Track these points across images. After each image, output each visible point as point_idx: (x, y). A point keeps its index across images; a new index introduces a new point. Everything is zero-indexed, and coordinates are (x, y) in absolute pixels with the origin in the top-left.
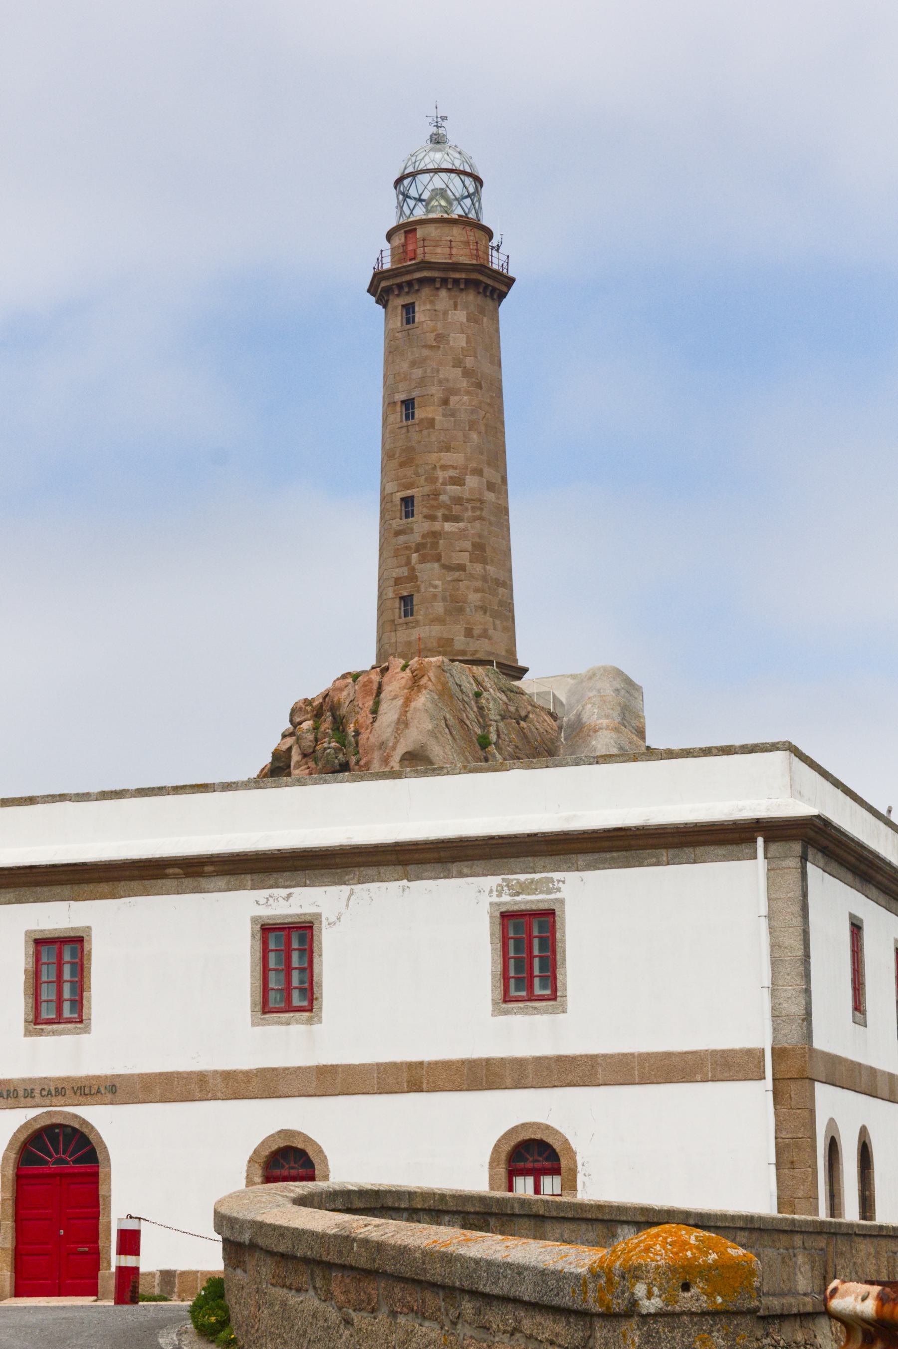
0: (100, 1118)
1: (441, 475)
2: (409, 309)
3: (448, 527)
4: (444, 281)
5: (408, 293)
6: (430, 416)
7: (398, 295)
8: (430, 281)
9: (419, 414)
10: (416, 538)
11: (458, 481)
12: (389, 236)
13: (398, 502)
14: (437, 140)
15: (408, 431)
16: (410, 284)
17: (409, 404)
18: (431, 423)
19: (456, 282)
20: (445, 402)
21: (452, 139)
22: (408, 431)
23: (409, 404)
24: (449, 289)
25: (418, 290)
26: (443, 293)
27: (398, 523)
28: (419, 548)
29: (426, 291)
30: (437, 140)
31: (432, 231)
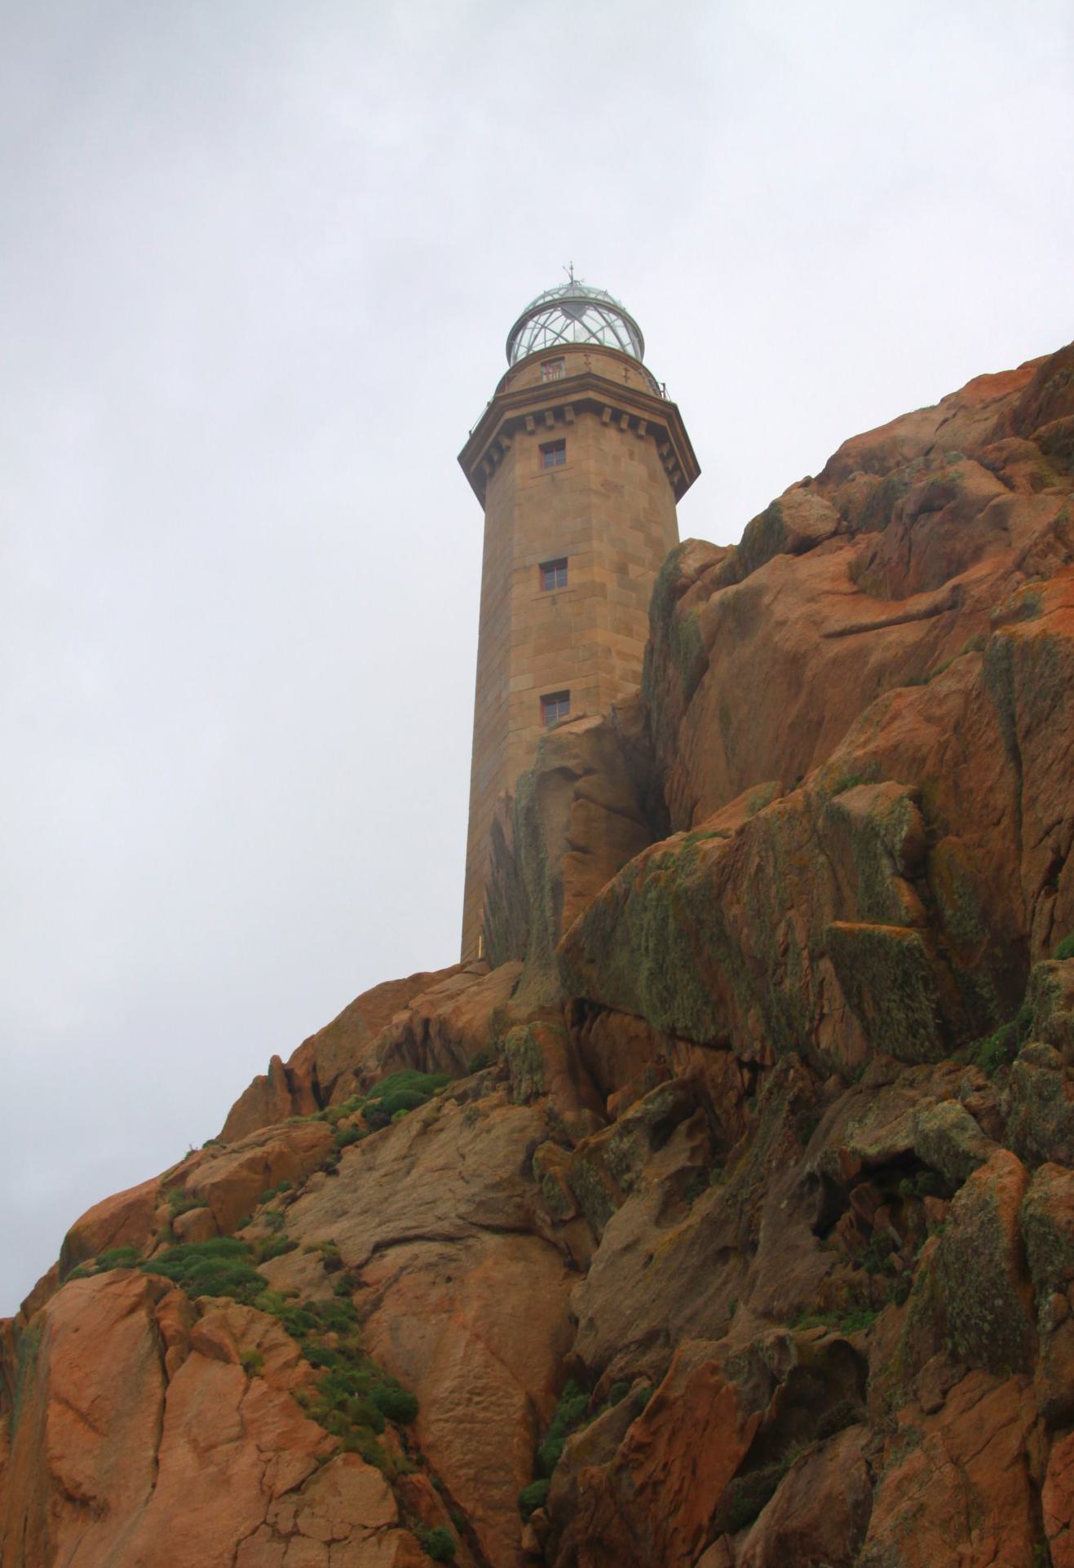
4: (617, 416)
5: (551, 428)
6: (598, 580)
7: (532, 433)
8: (595, 409)
13: (538, 702)
15: (554, 603)
16: (559, 413)
18: (598, 590)
19: (634, 423)
20: (622, 569)
22: (554, 603)
24: (622, 431)
25: (571, 423)
26: (612, 433)
29: (588, 423)
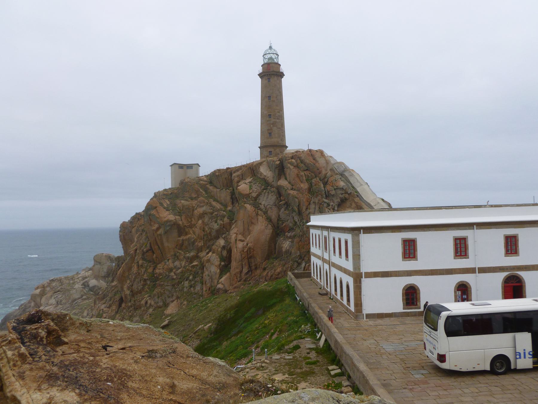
0: (523, 274)
1: (276, 111)
2: (269, 79)
3: (278, 120)
9: (272, 99)
10: (272, 122)
11: (279, 112)
12: (262, 66)
14: (270, 48)
17: (269, 97)
21: (273, 47)
23: (269, 97)
27: (268, 119)
28: (272, 124)
30: (270, 48)
31: (273, 65)
